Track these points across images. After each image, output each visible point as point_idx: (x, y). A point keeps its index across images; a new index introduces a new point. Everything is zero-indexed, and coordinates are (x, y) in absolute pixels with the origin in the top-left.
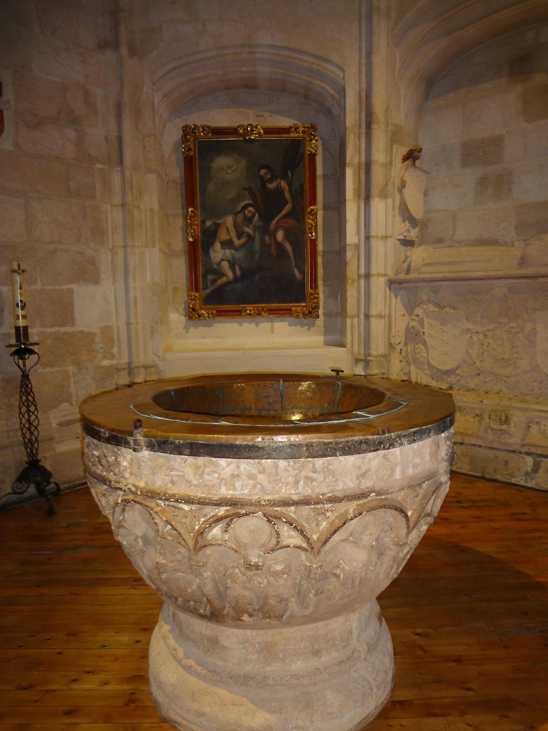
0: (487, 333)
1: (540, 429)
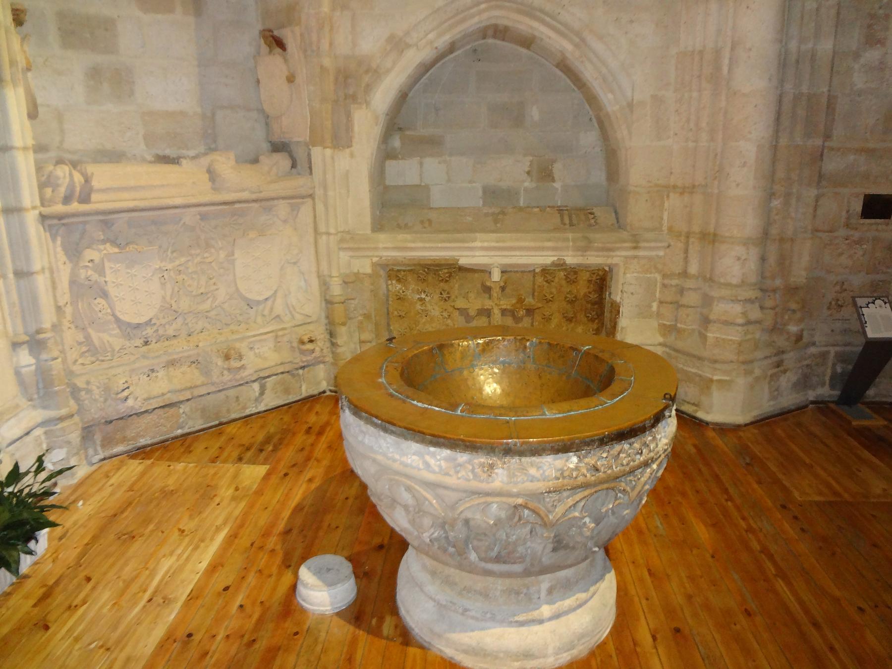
0: (180, 268)
1: (255, 354)
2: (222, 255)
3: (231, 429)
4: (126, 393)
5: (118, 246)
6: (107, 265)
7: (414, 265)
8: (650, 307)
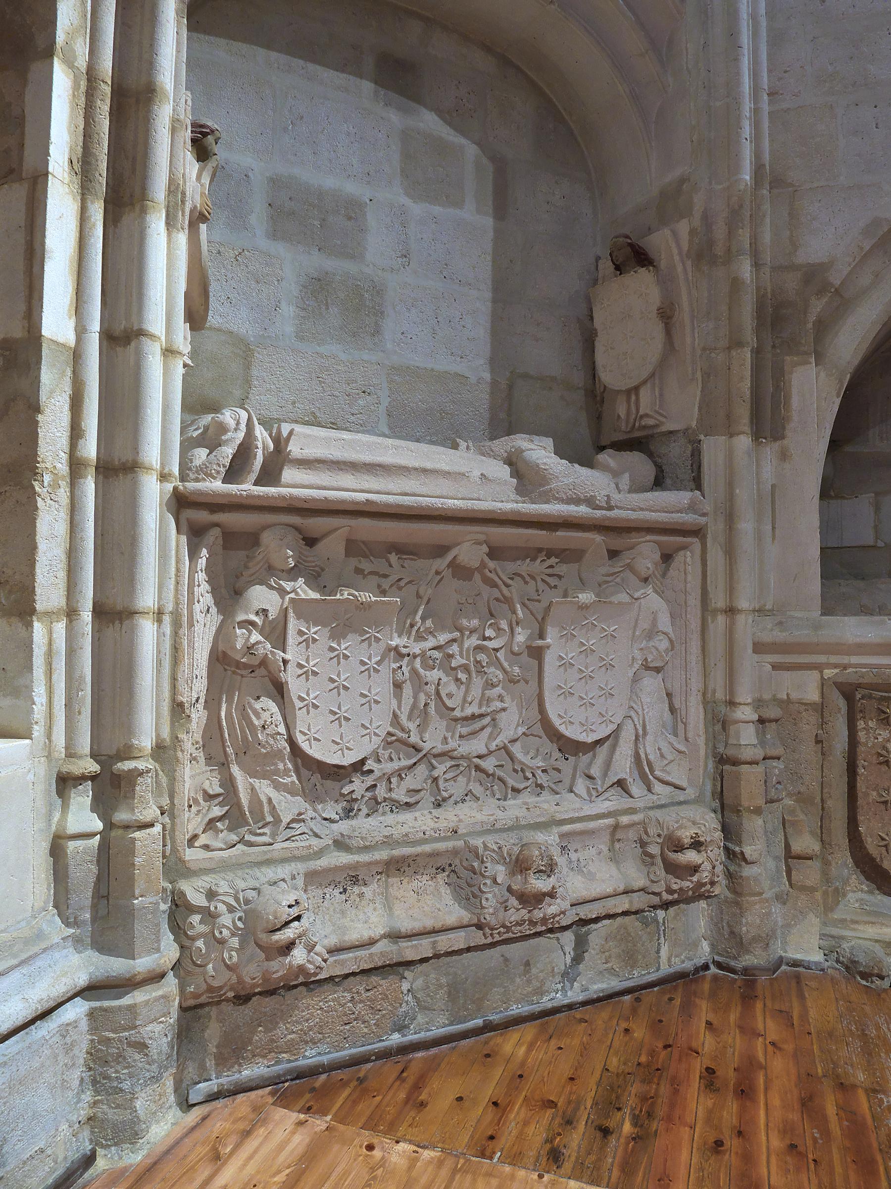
2: (521, 637)
3: (513, 1045)
4: (289, 933)
5: (322, 589)
6: (293, 624)
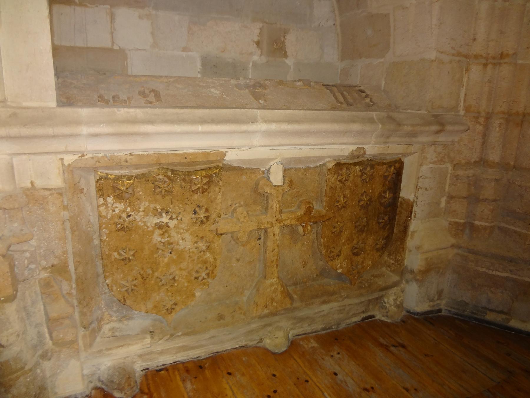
7: (149, 165)
8: (438, 203)
